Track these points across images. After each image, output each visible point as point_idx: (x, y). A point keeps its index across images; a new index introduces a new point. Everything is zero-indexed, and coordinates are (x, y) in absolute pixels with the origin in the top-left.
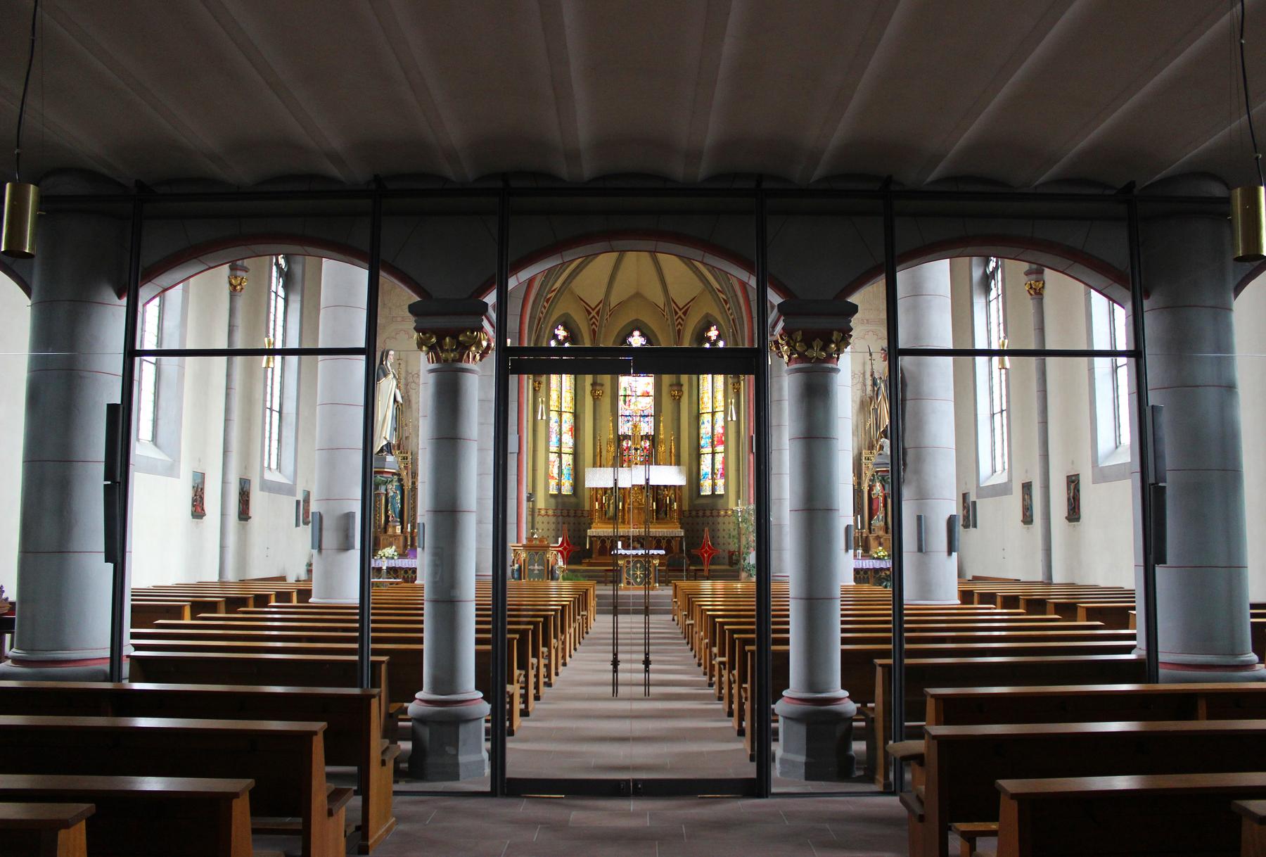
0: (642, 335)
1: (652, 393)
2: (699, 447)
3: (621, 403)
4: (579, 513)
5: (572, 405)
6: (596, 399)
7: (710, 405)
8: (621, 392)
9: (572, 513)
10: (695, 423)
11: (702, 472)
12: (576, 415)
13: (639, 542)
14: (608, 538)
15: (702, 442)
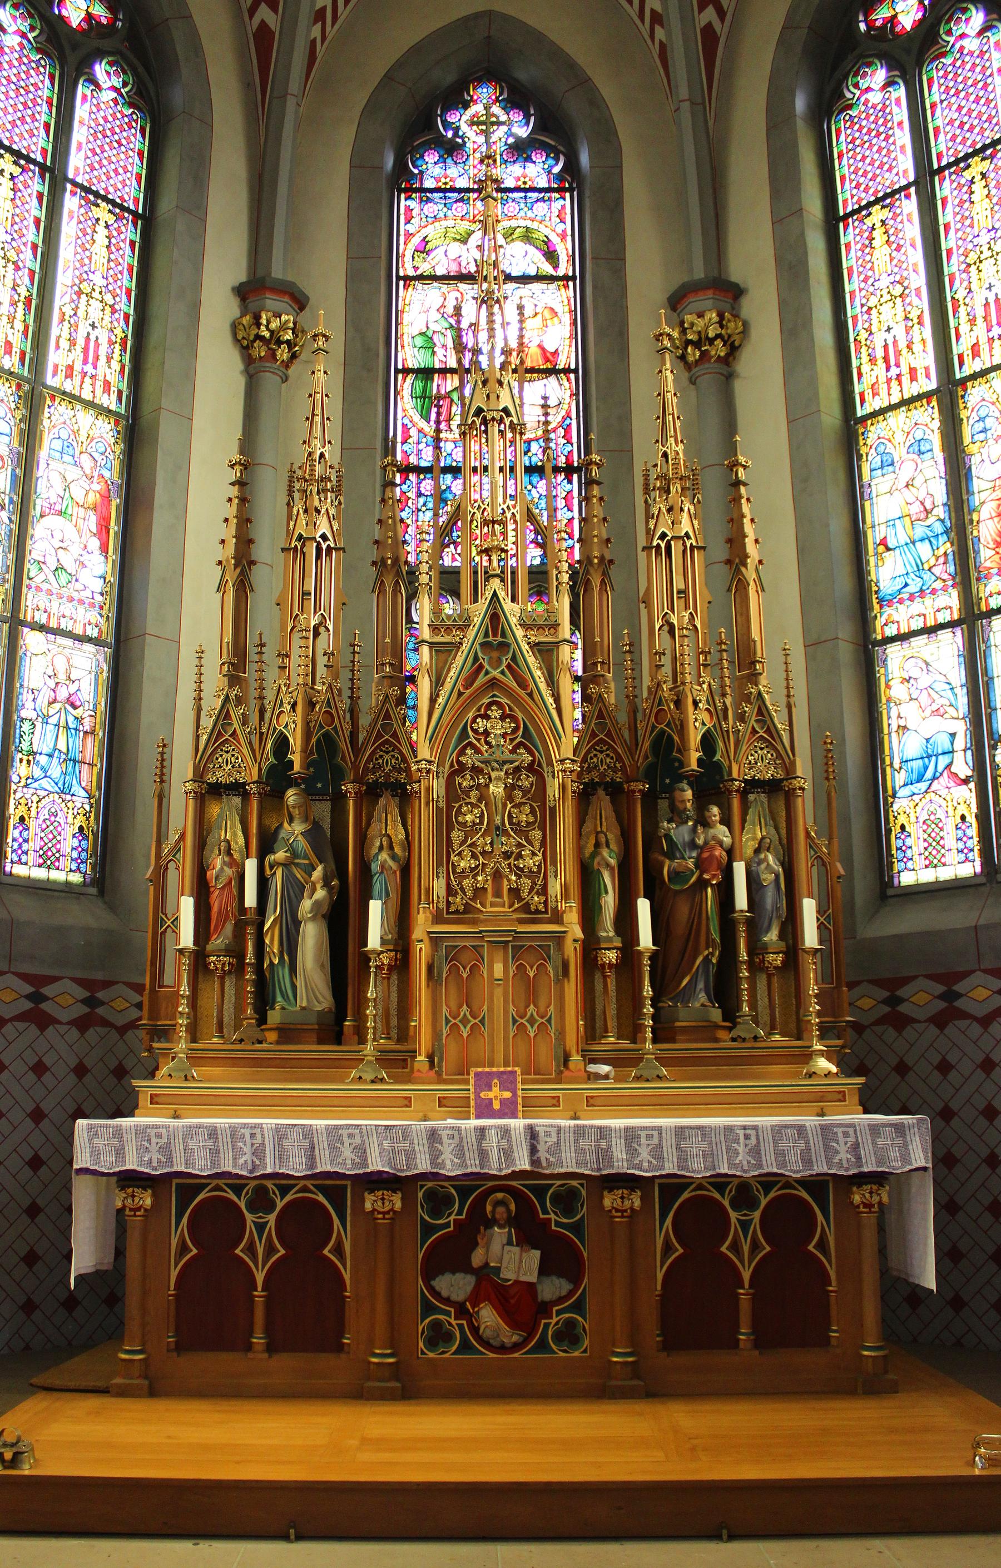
0: (517, 99)
1: (567, 358)
2: (862, 597)
3: (406, 407)
4: (119, 1003)
5: (112, 370)
6: (262, 358)
7: (925, 358)
8: (410, 356)
9: (65, 999)
10: (833, 464)
11: (903, 747)
12: (136, 433)
13: (528, 1231)
14: (263, 1190)
15: (886, 573)
